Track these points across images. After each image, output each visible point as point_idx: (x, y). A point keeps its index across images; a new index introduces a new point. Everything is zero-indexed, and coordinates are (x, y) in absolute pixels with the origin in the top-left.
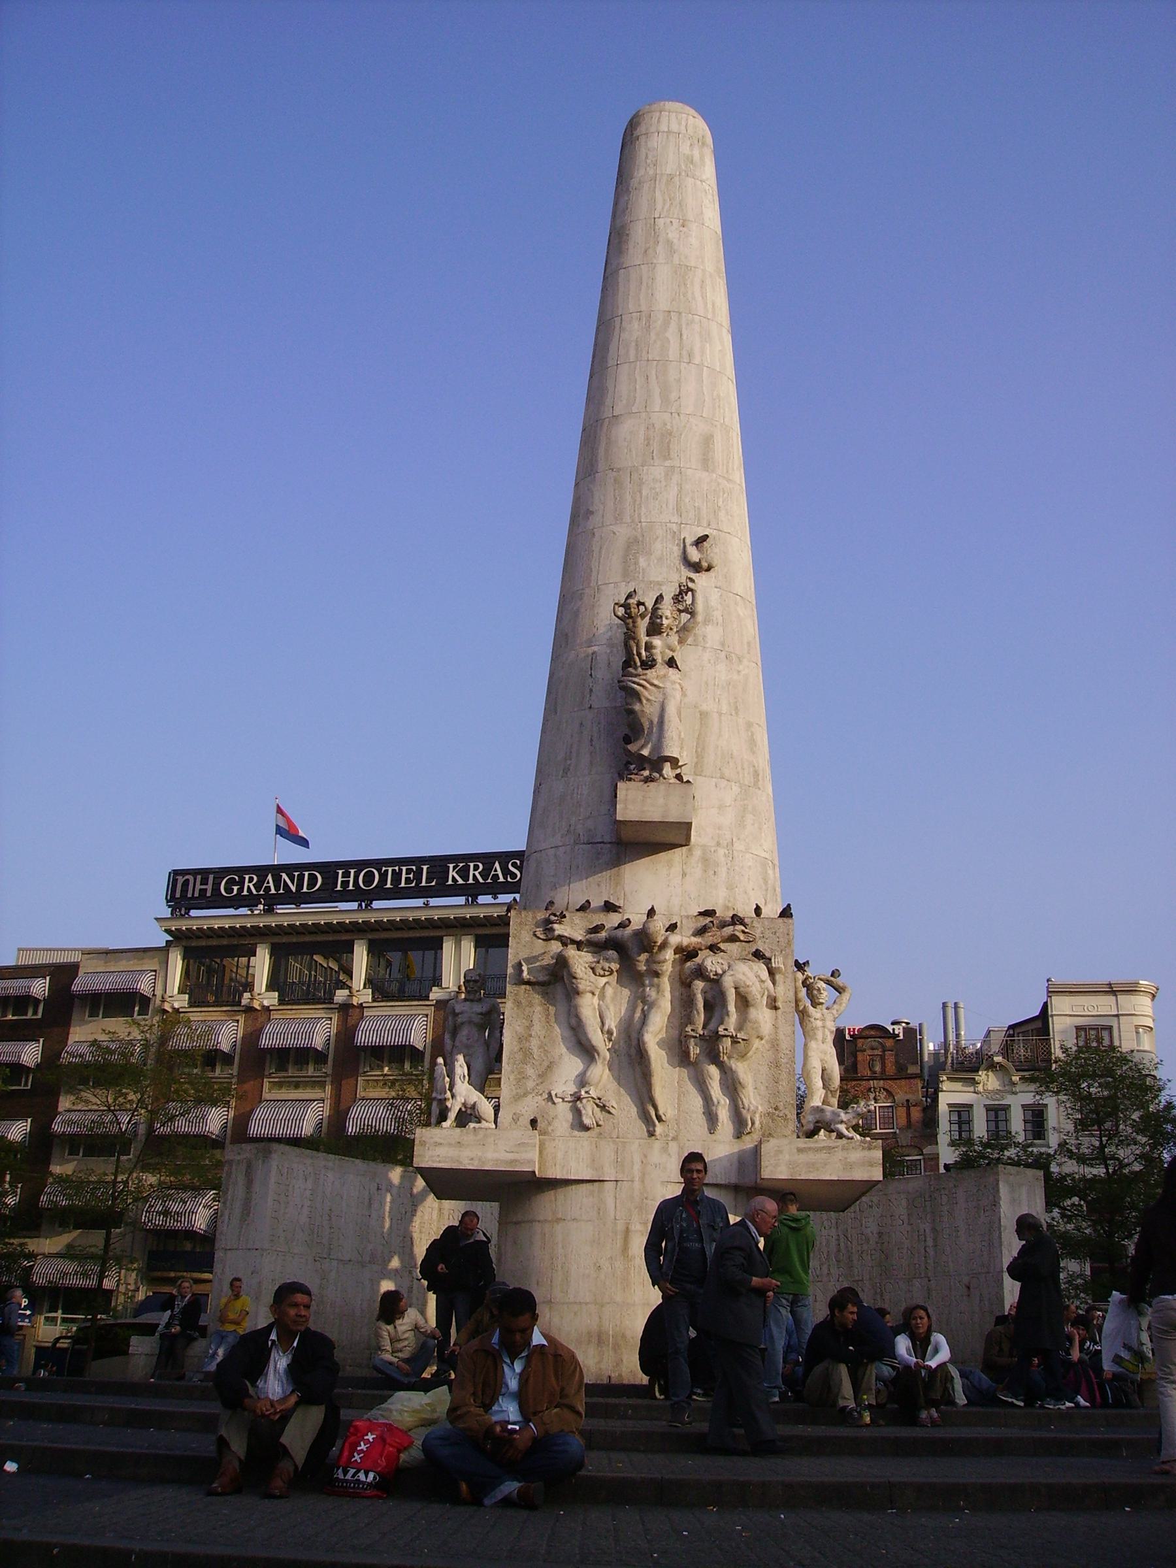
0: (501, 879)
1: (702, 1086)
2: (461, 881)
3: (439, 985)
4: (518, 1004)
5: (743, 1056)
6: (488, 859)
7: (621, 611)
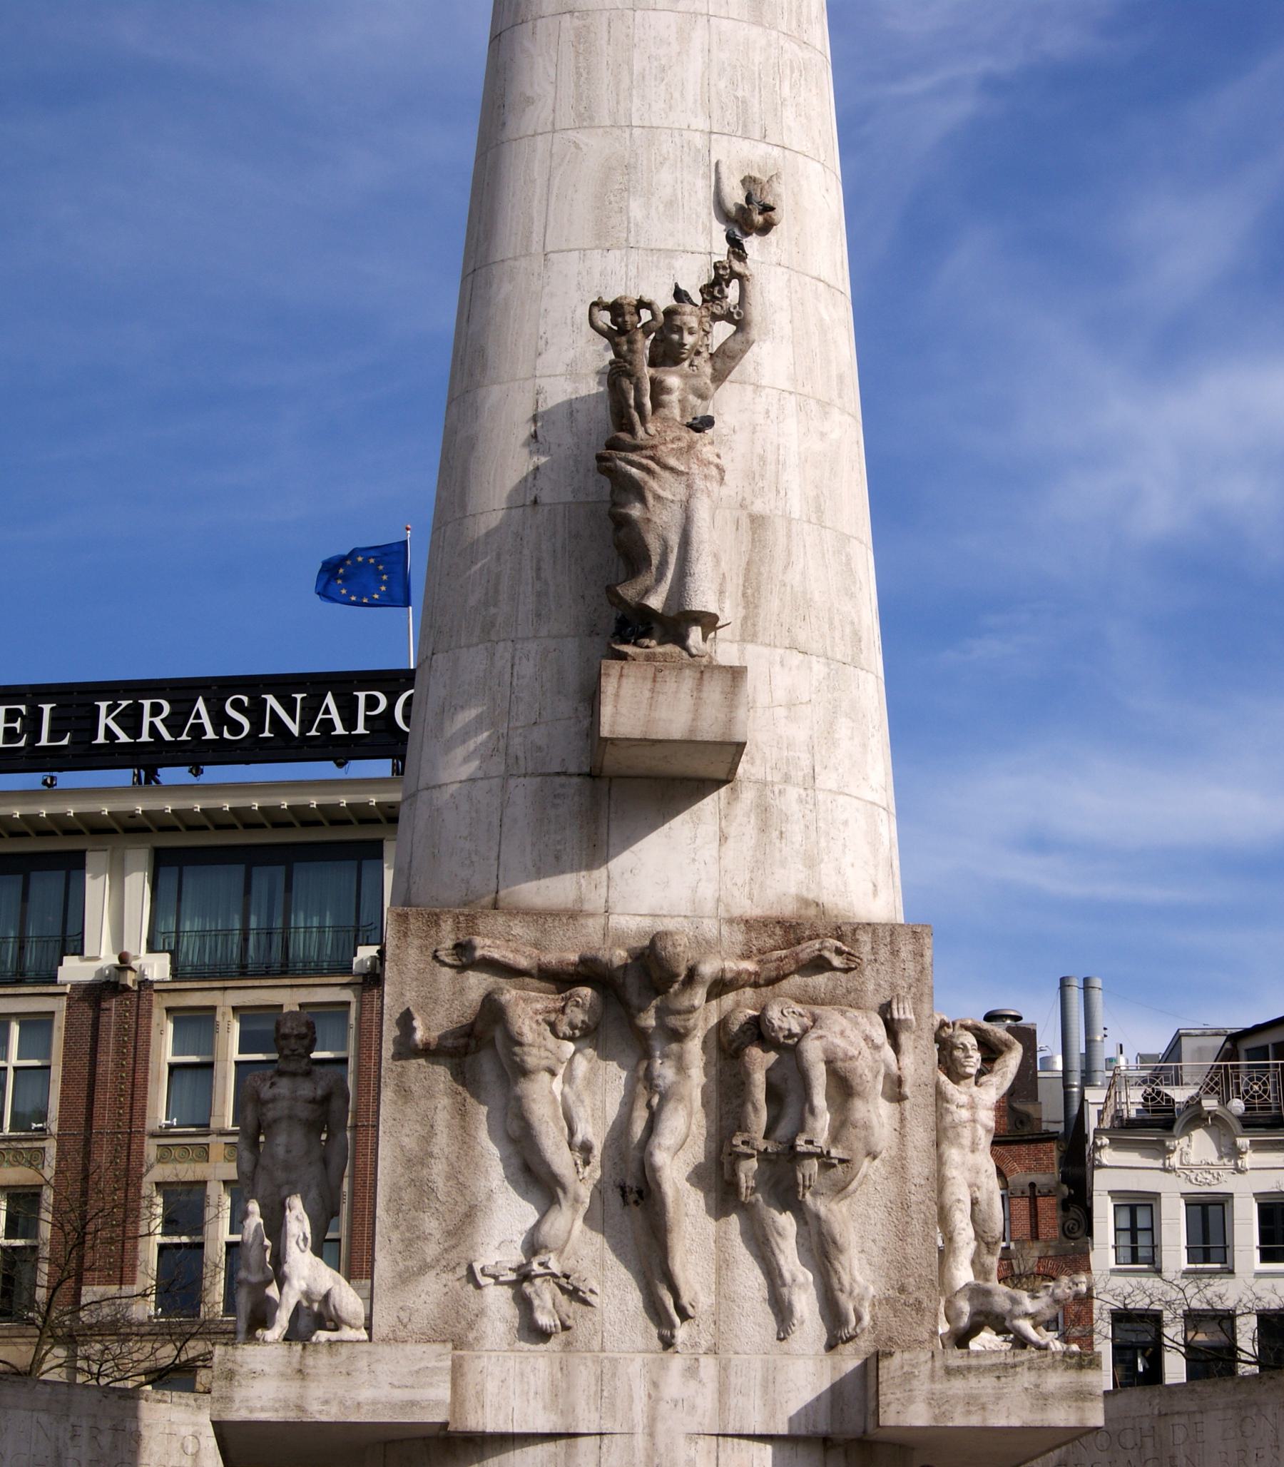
0: (210, 734)
2: (123, 738)
3: (80, 952)
4: (404, 1093)
5: (840, 1190)
6: (181, 692)
7: (605, 318)
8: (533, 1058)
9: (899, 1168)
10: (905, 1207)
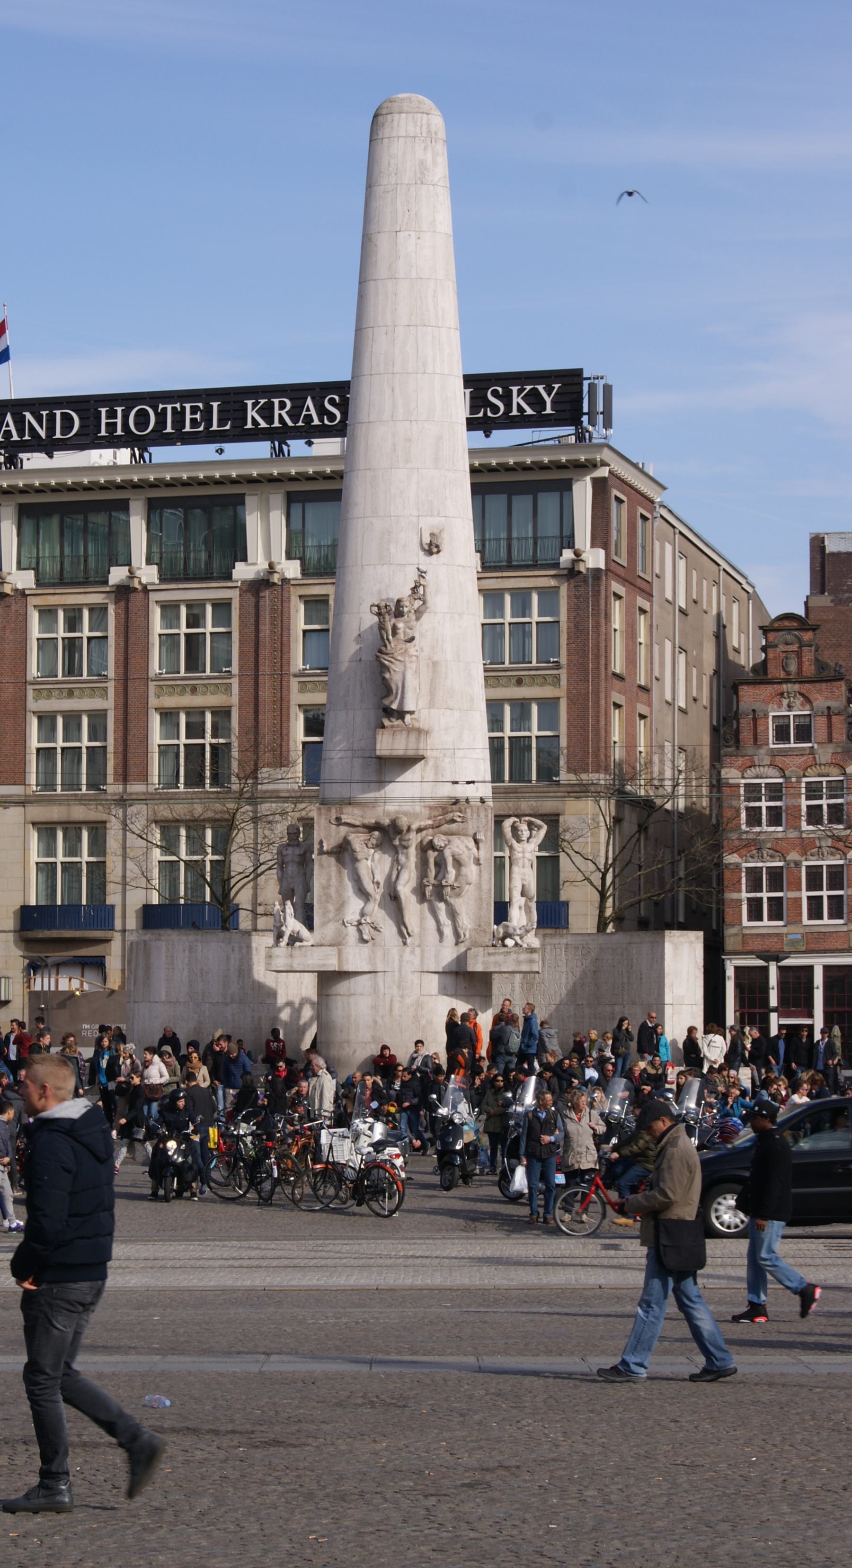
0: (316, 422)
1: (434, 913)
2: (263, 424)
3: (244, 559)
4: (321, 866)
5: (458, 895)
6: (297, 393)
7: (375, 609)
8: (360, 856)
9: (479, 887)
10: (481, 899)
